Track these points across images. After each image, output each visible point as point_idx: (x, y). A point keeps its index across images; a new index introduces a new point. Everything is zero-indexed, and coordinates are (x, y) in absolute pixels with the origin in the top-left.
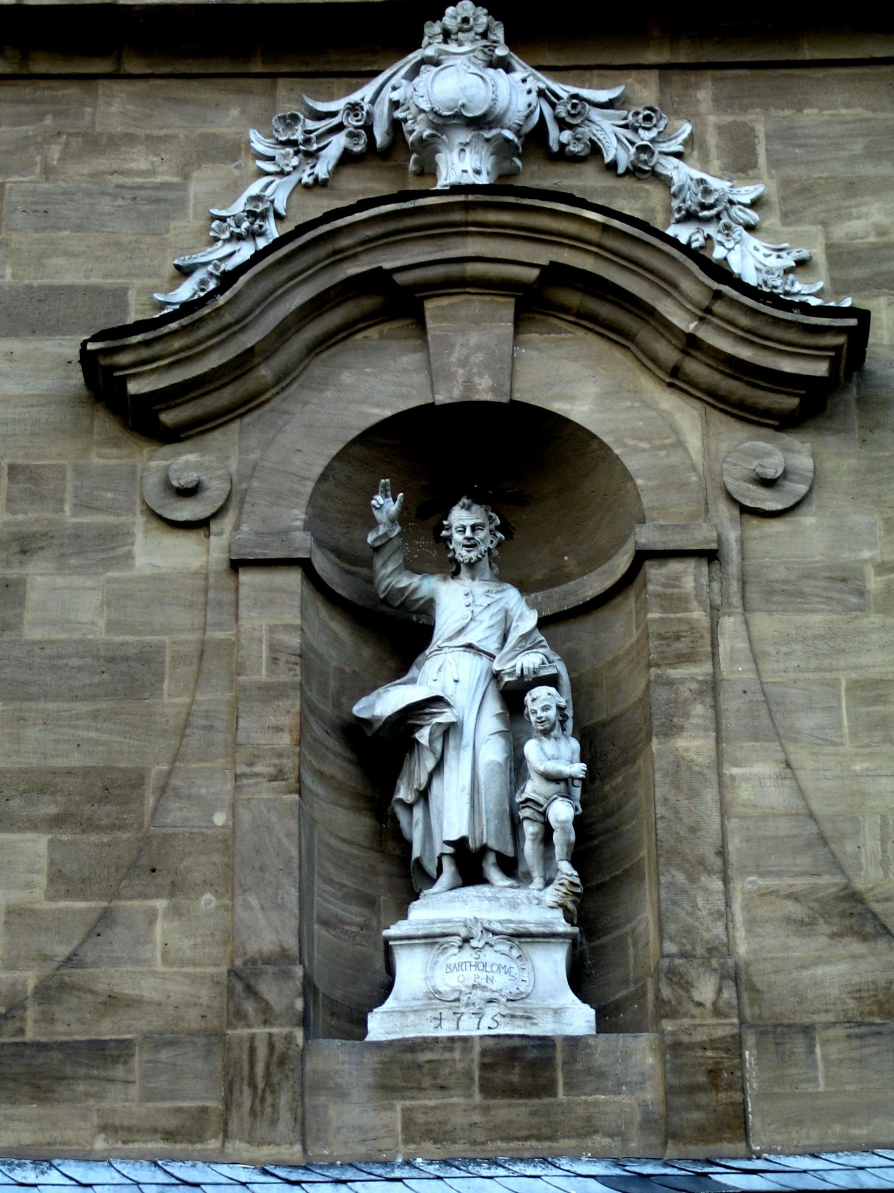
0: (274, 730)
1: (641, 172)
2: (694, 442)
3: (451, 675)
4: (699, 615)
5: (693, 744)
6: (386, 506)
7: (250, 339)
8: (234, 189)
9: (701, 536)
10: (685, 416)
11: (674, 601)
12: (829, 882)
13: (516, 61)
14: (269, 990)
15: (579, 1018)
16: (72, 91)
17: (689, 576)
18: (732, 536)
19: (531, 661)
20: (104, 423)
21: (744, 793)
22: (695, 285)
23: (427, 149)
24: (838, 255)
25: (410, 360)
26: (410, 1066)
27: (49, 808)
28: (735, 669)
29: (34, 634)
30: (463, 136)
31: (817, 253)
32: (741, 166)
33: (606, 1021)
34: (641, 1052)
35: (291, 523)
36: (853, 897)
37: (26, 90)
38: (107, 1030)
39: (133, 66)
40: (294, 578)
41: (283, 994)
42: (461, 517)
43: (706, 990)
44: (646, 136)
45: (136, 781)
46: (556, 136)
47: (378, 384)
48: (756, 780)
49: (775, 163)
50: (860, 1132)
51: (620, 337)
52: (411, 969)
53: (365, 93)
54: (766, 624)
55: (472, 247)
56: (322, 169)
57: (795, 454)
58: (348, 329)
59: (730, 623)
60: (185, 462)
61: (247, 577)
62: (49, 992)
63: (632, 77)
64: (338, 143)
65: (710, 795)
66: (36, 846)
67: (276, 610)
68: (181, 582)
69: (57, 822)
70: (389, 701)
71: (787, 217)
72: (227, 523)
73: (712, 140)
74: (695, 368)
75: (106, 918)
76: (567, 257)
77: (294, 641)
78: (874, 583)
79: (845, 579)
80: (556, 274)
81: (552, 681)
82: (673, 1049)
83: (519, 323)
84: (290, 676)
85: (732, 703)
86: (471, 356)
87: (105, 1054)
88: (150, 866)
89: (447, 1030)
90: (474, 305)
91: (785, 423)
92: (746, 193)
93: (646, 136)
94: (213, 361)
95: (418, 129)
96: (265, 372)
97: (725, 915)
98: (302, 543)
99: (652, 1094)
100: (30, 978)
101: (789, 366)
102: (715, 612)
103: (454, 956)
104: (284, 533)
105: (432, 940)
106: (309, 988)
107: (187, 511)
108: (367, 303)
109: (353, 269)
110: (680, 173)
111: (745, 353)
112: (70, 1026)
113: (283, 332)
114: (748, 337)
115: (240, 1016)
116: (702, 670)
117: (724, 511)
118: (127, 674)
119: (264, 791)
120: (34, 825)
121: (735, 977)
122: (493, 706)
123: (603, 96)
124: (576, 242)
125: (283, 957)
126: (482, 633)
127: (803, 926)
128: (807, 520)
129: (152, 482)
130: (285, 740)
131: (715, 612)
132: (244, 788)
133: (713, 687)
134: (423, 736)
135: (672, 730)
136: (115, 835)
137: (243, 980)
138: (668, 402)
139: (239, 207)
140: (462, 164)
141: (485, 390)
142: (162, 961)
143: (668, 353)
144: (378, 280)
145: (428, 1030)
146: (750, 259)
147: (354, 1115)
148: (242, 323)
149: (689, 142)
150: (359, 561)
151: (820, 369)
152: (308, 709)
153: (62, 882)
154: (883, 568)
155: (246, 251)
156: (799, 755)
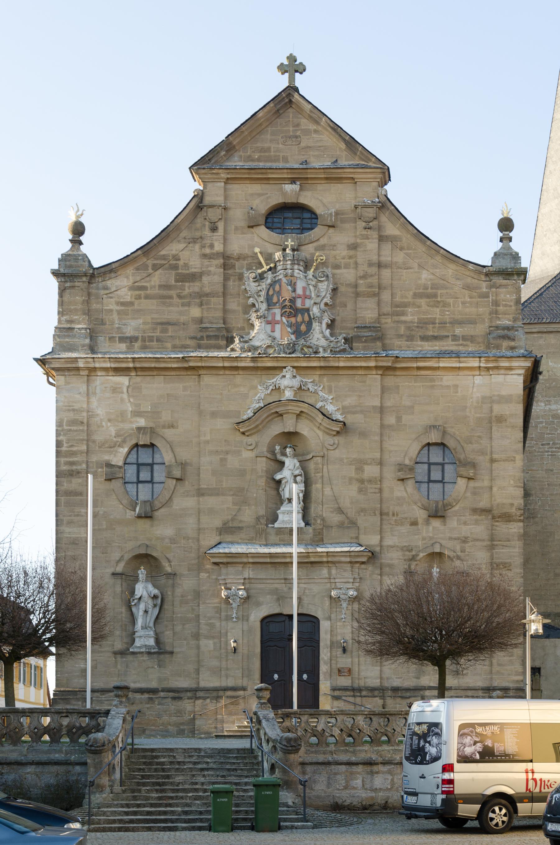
0: (262, 482)
1: (316, 392)
2: (321, 438)
3: (285, 474)
4: (321, 466)
5: (319, 486)
6: (278, 448)
7: (258, 423)
8: (256, 395)
9: (322, 454)
10: (320, 433)
11: (316, 464)
12: (336, 506)
13: (298, 376)
14: (261, 520)
15: (303, 524)
16: (232, 377)
17: (319, 460)
18: (326, 453)
19: (297, 472)
20: (238, 433)
21: (326, 493)
22: (321, 416)
23: (284, 390)
24: (344, 408)
25: (281, 424)
26: (280, 531)
27: (232, 493)
28: (326, 474)
29: (229, 466)
30: (288, 389)
31: (341, 407)
32: (330, 392)
33: (307, 524)
34: (310, 529)
35: (264, 449)
36: (340, 508)
37: (225, 377)
38: (240, 525)
39: (241, 372)
40: (264, 459)
41: (263, 521)
42: (288, 450)
43: (319, 521)
44: (316, 388)
45: (243, 489)
46: (303, 387)
47: (276, 428)
48: (328, 491)
49: (335, 392)
50: (338, 541)
51: (312, 421)
52: (281, 517)
53: (275, 380)
54: (330, 467)
55: (290, 408)
56: (269, 392)
57: (336, 439)
58: (273, 419)
59: (325, 467)
60: (250, 440)
61: (258, 459)
62: (233, 520)
63: (315, 376)
64: (271, 388)
65: (321, 493)
66: (230, 498)
67: (263, 465)
68: (249, 456)
69: (233, 495)
70: (278, 477)
71: (337, 401)
72: (255, 450)
73: (326, 387)
74: (321, 427)
75: (240, 509)
76: (303, 410)
77: (265, 469)
78: (345, 461)
79: (341, 460)
80: (302, 412)
81: (301, 475)
82: (314, 529)
83: (297, 419)
84: (264, 474)
85: (325, 479)
86: (289, 425)
87: (240, 528)
88: (245, 502)
89: (285, 526)
90: (290, 416)
91: (334, 435)
92: (331, 397)
93: (316, 388)
94: (253, 426)
95: (282, 387)
96: (260, 427)
97: (322, 511)
98: (266, 454)
99: (311, 535)
100: (230, 517)
101: (334, 429)
102: (323, 465)
103: (286, 515)
104: (263, 452)
105: (283, 513)
106: (267, 519)
107: (250, 448)
108: (276, 415)
109: (273, 411)
110: (321, 393)
111: (328, 426)
112: (236, 524)
113: (263, 421)
114: (328, 424)
115: (257, 524)
116: (321, 474)
117: (325, 450)
118: (242, 473)
119: (260, 491)
120: (230, 495)
121: (323, 520)
122: (293, 478)
123: (310, 381)
124: (305, 408)
125: (263, 516)
126: (291, 467)
127: (332, 512)
128: (337, 451)
129: (245, 443)
130: (264, 484)
131: (323, 465)
132: (259, 490)
133: (322, 476)
134: (283, 482)
135: (316, 483)
136: (241, 497)
137: (258, 519)
138: (318, 431)
139: (257, 398)
140: (288, 394)
141: (292, 430)
142: (248, 516)
143: (318, 425)
144: (277, 412)
145: (282, 526)
146: (330, 408)
147: (273, 538)
148: (257, 420)
149: (324, 387)
150: (273, 453)
151: (338, 429)
152: (267, 477)
153: (234, 504)
154: (347, 458)
155: (257, 406)
156: (333, 487)
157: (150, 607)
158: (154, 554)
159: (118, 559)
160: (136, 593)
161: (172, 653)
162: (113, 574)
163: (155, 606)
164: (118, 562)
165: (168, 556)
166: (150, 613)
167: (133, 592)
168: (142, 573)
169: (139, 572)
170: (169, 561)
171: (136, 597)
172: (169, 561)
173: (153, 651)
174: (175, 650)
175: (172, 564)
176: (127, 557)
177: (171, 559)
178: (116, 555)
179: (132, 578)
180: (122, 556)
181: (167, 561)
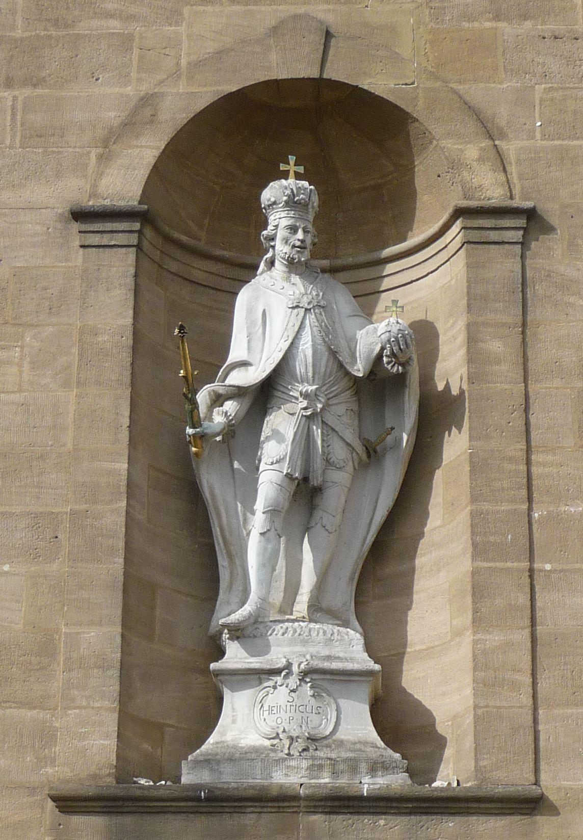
157: (339, 452)
158: (379, 83)
159: (113, 116)
160: (237, 352)
161: (530, 804)
162: (80, 215)
163: (372, 454)
164: (111, 141)
165: (475, 92)
166: (333, 499)
167: (213, 353)
168: (282, 203)
169: (272, 193)
170: (489, 130)
171: (237, 378)
172: (489, 130)
173: (368, 784)
174: (552, 783)
175: (511, 148)
176: (186, 98)
177: (502, 114)
178: (106, 96)
179: (200, 269)
180: (147, 100)
181: (471, 126)
